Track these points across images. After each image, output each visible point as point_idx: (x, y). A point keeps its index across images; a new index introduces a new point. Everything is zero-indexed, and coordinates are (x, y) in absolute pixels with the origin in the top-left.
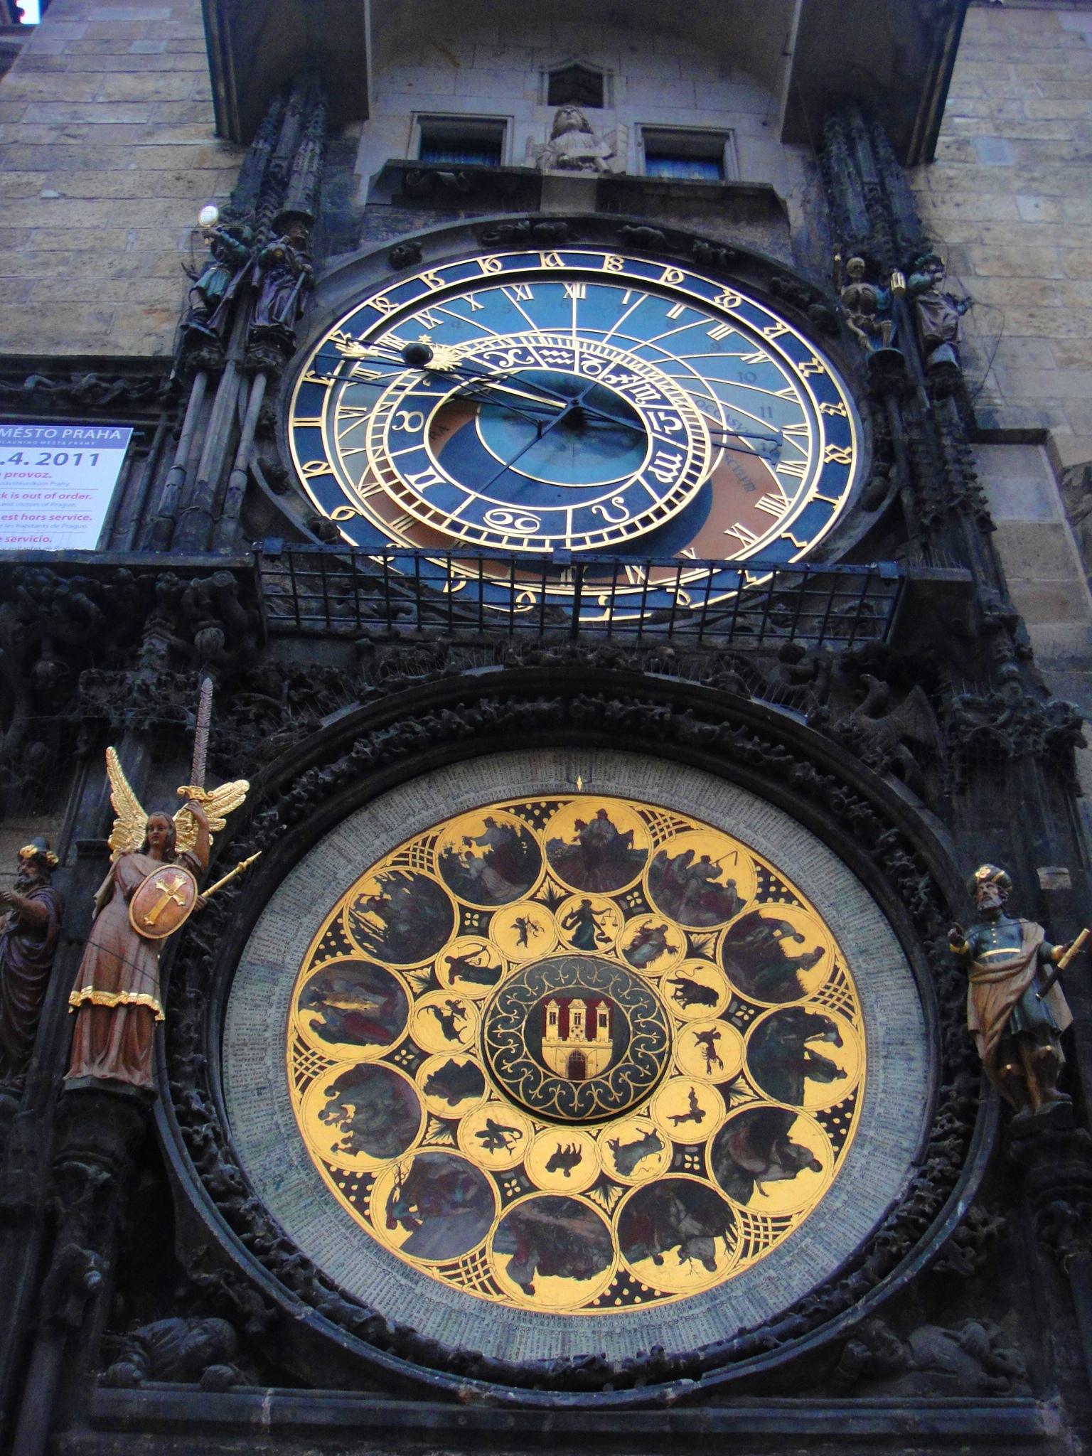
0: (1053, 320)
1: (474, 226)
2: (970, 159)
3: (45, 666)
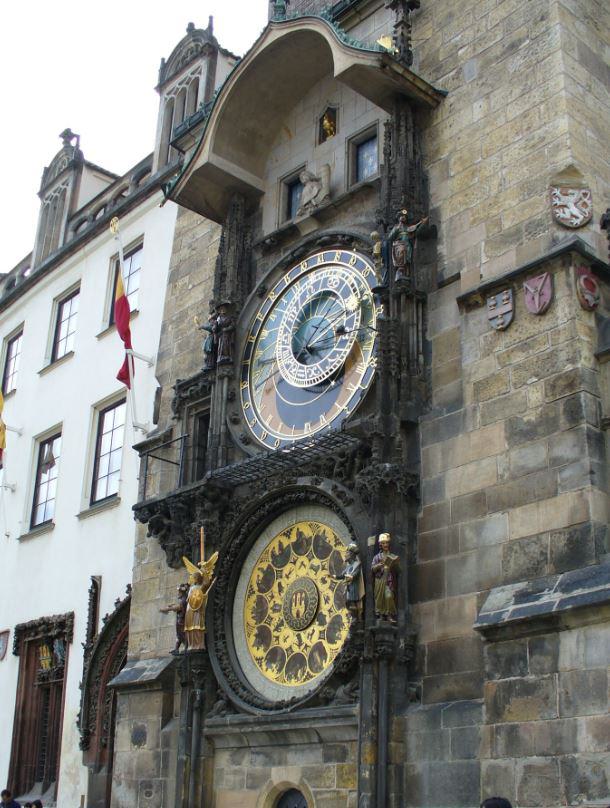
1: (278, 265)
3: (183, 523)
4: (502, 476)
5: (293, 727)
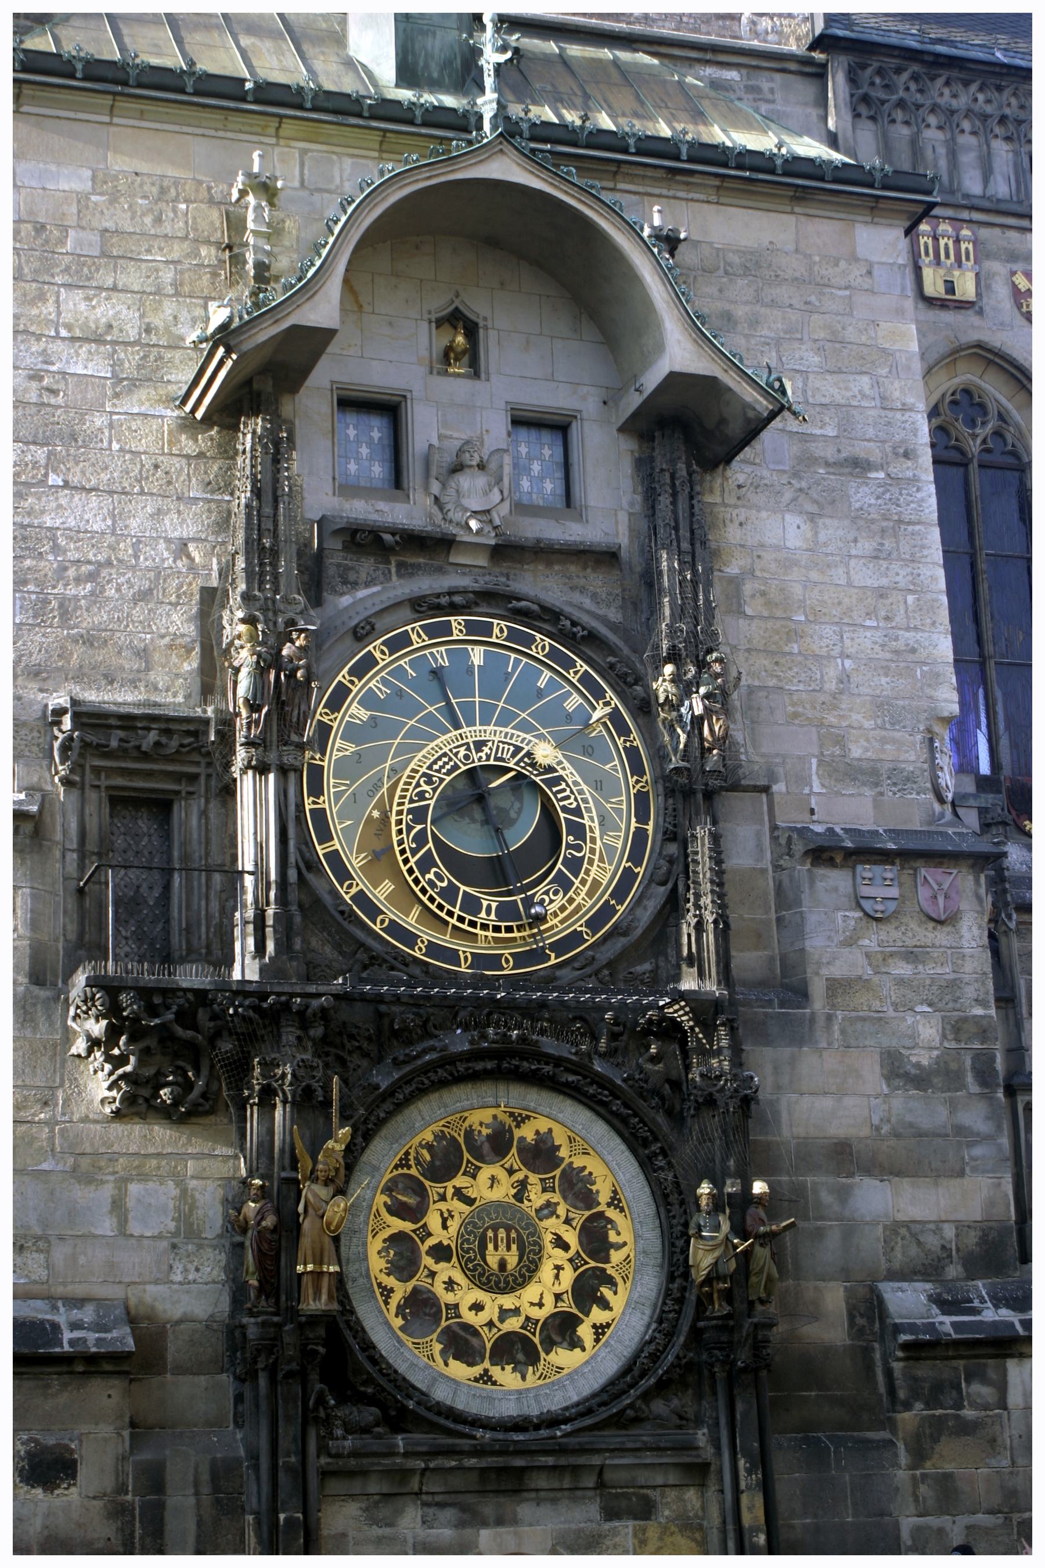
0: (790, 669)
1: (410, 600)
2: (757, 461)
3: (226, 1046)
4: (878, 1129)
5: (563, 1461)
